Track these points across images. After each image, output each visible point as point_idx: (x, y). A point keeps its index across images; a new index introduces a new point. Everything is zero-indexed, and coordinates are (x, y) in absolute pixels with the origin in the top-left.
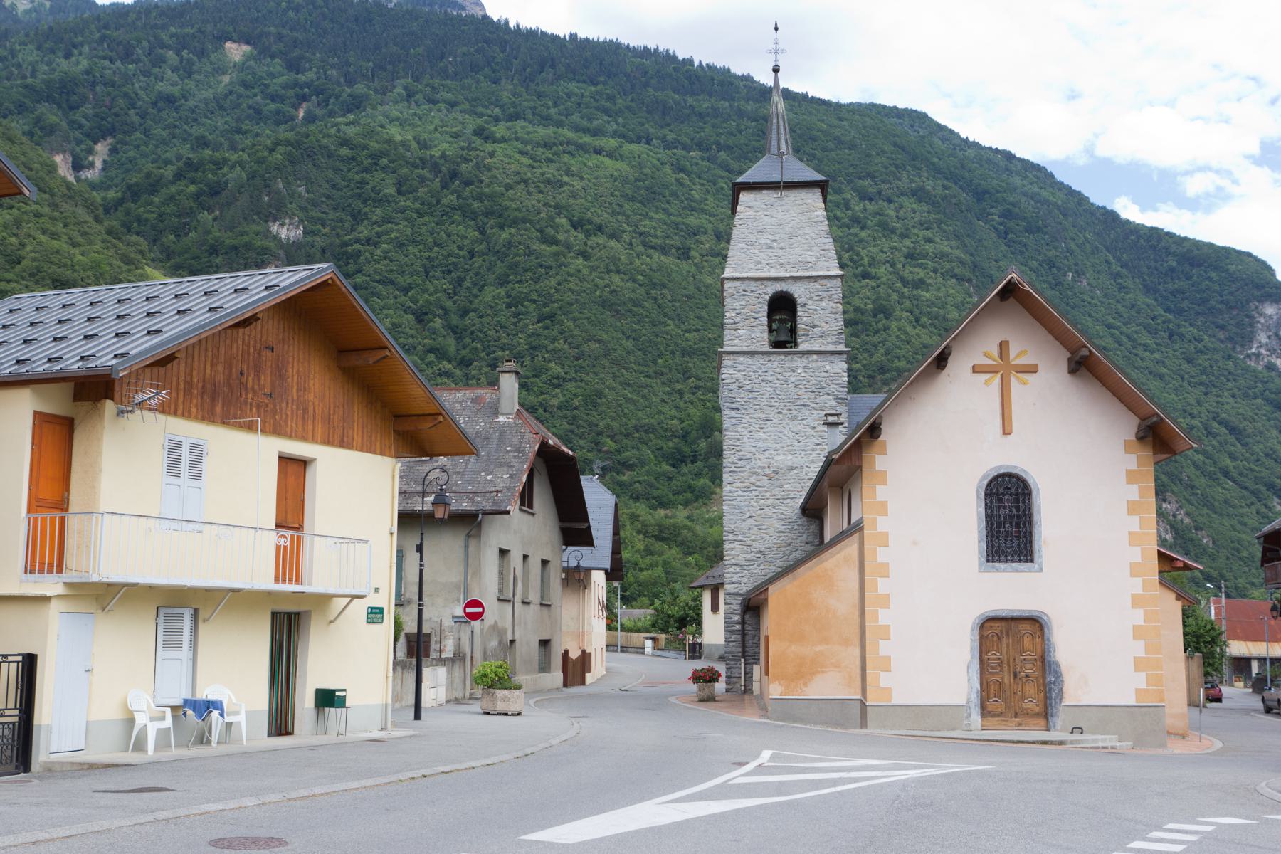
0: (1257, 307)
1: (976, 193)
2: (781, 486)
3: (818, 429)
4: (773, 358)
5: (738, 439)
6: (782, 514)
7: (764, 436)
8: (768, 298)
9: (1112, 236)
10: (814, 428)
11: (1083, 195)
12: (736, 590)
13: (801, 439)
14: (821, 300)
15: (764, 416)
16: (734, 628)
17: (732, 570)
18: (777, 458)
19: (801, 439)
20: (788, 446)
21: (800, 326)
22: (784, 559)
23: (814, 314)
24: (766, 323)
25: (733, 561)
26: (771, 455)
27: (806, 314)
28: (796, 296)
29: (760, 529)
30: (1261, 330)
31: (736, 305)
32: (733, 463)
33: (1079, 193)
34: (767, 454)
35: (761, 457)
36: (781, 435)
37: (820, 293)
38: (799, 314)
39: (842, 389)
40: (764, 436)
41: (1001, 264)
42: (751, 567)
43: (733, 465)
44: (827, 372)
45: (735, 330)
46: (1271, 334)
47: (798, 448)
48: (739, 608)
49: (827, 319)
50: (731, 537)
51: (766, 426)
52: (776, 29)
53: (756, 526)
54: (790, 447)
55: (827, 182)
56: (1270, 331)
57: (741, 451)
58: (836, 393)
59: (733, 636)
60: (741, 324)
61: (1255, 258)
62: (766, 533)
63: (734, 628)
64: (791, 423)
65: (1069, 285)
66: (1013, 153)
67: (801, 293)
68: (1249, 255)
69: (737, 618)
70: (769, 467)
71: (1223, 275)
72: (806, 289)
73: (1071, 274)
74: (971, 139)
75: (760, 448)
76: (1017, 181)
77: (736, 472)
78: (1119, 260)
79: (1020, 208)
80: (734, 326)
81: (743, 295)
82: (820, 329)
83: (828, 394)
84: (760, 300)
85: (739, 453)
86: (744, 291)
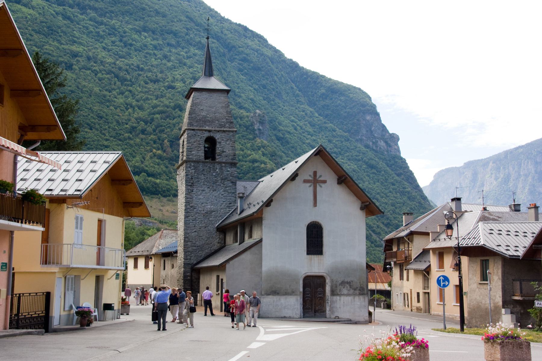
5: (191, 198)
8: (205, 138)
14: (227, 141)
21: (217, 151)
25: (188, 250)
38: (217, 146)
44: (229, 171)
60: (194, 149)
83: (229, 181)
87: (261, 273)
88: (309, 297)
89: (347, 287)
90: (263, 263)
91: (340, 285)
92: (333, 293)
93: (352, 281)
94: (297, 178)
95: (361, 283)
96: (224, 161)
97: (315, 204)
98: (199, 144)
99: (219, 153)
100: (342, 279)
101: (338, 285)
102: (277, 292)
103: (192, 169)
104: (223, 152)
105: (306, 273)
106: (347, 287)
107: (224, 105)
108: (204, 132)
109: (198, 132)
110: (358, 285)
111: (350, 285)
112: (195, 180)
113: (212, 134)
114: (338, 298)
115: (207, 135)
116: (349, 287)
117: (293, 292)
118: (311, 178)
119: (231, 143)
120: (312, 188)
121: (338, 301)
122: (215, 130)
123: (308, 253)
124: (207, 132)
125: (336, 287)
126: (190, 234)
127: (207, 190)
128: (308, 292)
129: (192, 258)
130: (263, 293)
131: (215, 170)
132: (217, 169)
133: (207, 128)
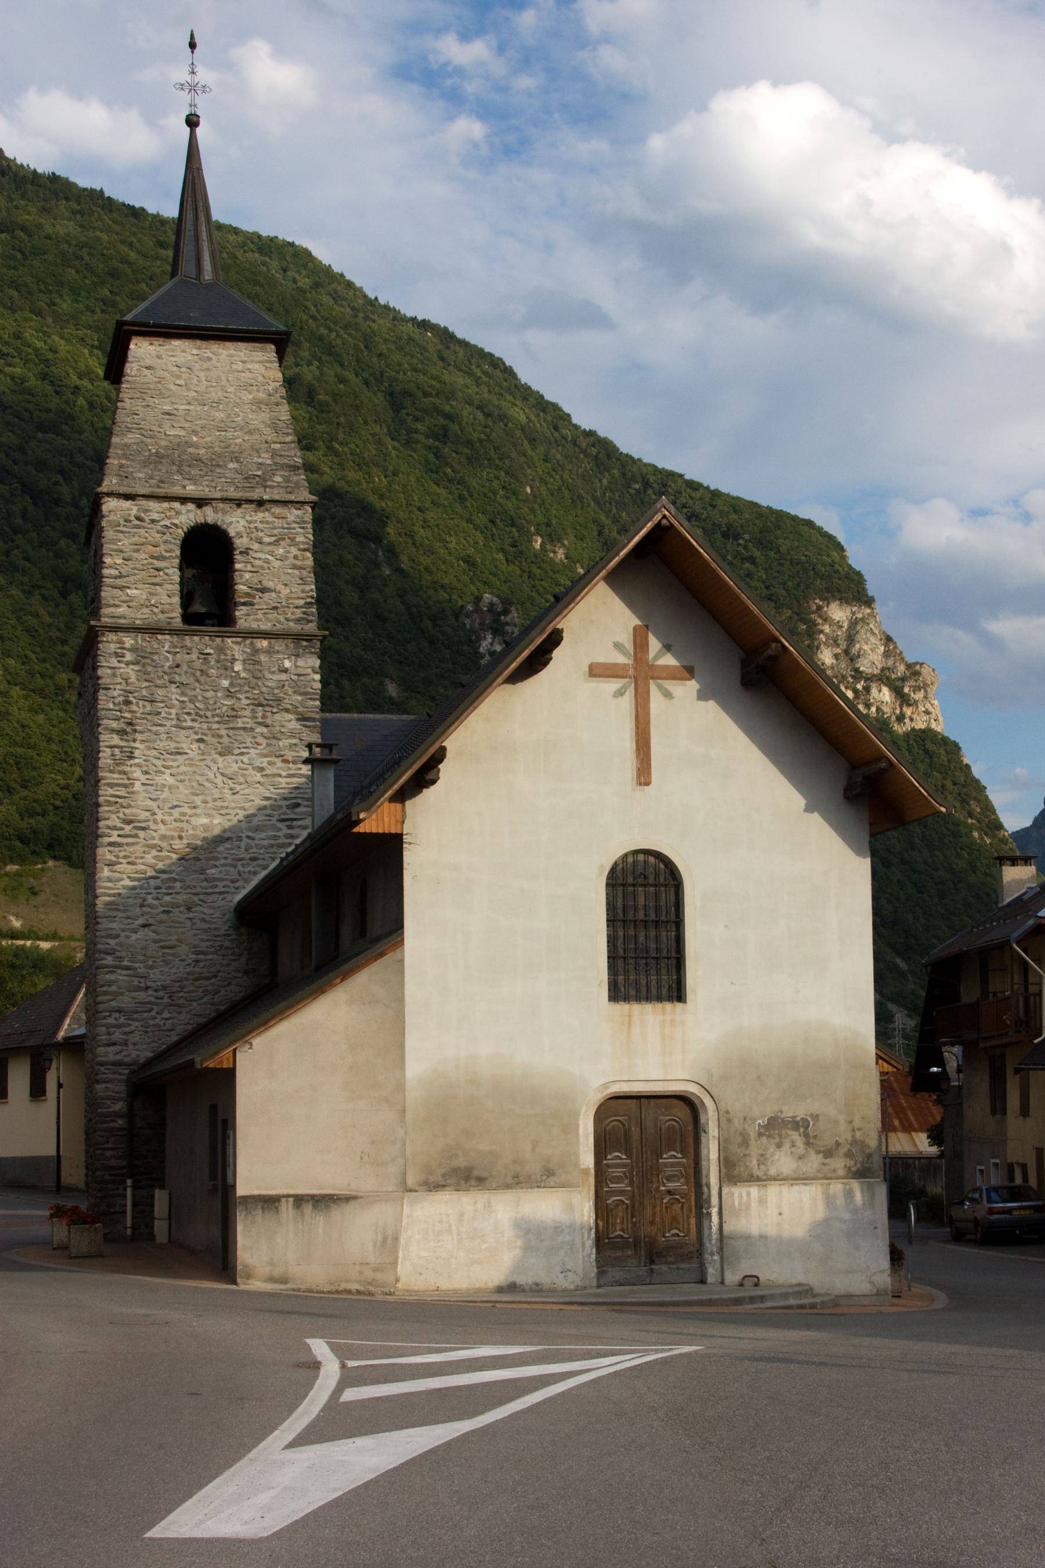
0: (819, 608)
1: (391, 394)
2: (203, 871)
3: (268, 772)
4: (188, 641)
5: (125, 786)
6: (203, 920)
7: (171, 780)
8: (181, 533)
9: (605, 481)
10: (262, 769)
11: (560, 409)
12: (119, 1057)
13: (238, 788)
14: (276, 543)
15: (173, 745)
16: (112, 1125)
17: (110, 1021)
18: (195, 821)
19: (238, 788)
20: (215, 800)
21: (241, 588)
22: (205, 1000)
23: (262, 567)
24: (178, 580)
25: (114, 1004)
26: (184, 814)
27: (249, 568)
28: (232, 534)
29: (162, 947)
30: (825, 644)
31: (125, 543)
32: (115, 828)
33: (555, 407)
34: (176, 813)
35: (167, 818)
36: (201, 779)
37: (275, 532)
38: (237, 566)
39: (311, 703)
40: (171, 780)
41: (430, 515)
42: (146, 1015)
43: (116, 833)
45: (122, 588)
46: (838, 651)
47: (233, 805)
48: (122, 1087)
49: (288, 577)
50: (109, 960)
51: (175, 764)
52: (193, 46)
53: (155, 941)
54: (219, 803)
55: (288, 334)
56: (838, 646)
57: (129, 806)
58: (301, 709)
59: (112, 1140)
60: (131, 578)
61: (820, 530)
62: (173, 955)
63: (112, 1125)
64: (220, 759)
65: (536, 556)
66: (451, 329)
67: (241, 529)
68: (809, 523)
69: (119, 1107)
70: (180, 838)
71: (772, 554)
72: (250, 522)
73: (539, 540)
74: (382, 301)
75: (164, 801)
76: (459, 380)
77: (120, 845)
78: (616, 520)
79: (460, 424)
80: (120, 582)
81: (137, 527)
82: (273, 595)
83: (287, 711)
84: (167, 537)
85: (126, 811)
86: (138, 518)
87: (401, 1087)
88: (622, 1192)
89: (793, 1145)
90: (411, 1043)
91: (760, 1135)
92: (732, 1173)
93: (816, 1117)
94: (557, 653)
95: (856, 1125)
96: (266, 626)
97: (643, 774)
98: (157, 558)
99: (248, 595)
100: (770, 1110)
101: (753, 1135)
102: (475, 1173)
103: (127, 664)
104: (264, 590)
105: (606, 1085)
106: (793, 1145)
107: (262, 395)
108: (176, 505)
109: (152, 504)
110: (844, 1134)
111: (806, 1135)
112: (139, 708)
113: (210, 515)
114: (754, 1191)
115: (188, 516)
116: (800, 1142)
117: (549, 1173)
118: (621, 659)
119: (294, 551)
120: (627, 702)
121: (754, 1205)
122: (224, 500)
123: (616, 994)
124: (191, 506)
125: (745, 1143)
126: (122, 939)
127: (193, 749)
128: (618, 1172)
129: (134, 1038)
130: (411, 1181)
131: (226, 667)
132: (234, 660)
133: (191, 489)
